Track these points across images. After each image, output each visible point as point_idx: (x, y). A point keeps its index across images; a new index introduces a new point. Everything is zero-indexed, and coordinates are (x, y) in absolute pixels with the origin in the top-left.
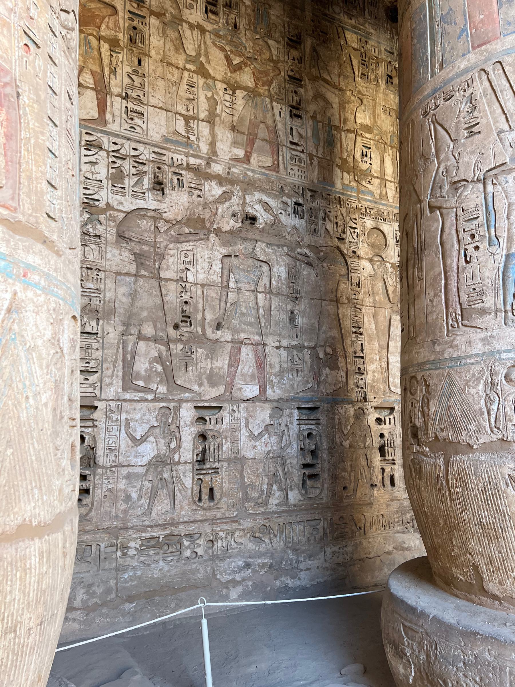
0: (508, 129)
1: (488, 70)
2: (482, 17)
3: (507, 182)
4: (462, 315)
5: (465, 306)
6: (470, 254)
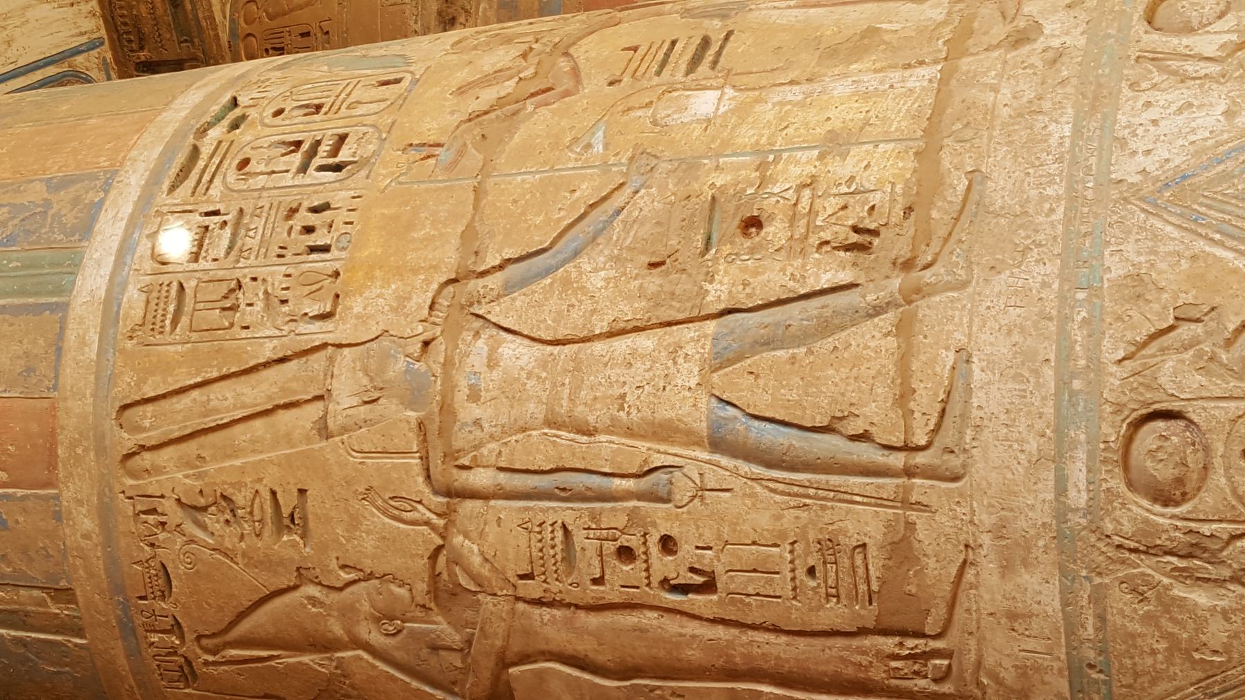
0: (320, 405)
3: (477, 423)
4: (904, 633)
5: (868, 614)
6: (683, 571)
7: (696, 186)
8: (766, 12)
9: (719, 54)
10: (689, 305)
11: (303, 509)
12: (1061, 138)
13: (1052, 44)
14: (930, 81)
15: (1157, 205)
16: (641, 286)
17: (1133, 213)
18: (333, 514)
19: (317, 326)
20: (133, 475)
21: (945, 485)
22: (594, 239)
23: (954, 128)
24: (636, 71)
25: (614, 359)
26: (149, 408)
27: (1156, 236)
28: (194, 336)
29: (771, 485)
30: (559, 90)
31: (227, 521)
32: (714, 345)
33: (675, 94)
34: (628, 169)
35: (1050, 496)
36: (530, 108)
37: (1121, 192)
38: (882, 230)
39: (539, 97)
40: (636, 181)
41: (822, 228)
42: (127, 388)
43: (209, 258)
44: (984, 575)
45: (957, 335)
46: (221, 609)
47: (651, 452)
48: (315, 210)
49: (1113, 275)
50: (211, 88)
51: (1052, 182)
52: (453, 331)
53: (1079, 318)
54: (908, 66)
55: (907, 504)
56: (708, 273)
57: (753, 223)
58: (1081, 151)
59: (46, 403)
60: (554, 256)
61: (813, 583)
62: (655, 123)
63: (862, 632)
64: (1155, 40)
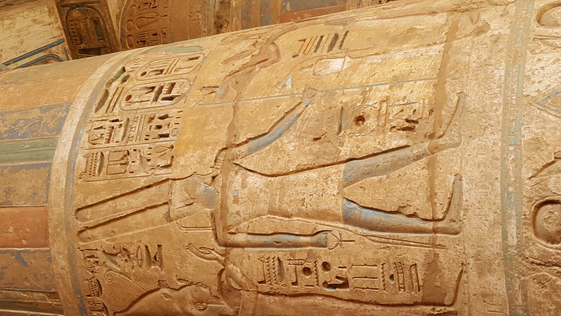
0: (166, 207)
1: (81, 226)
2: (11, 230)
3: (238, 213)
4: (435, 304)
5: (418, 296)
6: (333, 278)
7: (334, 103)
8: (363, 22)
9: (343, 41)
10: (332, 157)
11: (160, 254)
12: (500, 76)
13: (494, 33)
14: (439, 52)
15: (545, 106)
16: (310, 149)
17: (534, 110)
18: (174, 256)
19: (164, 171)
20: (83, 240)
21: (451, 236)
22: (288, 128)
23: (451, 73)
24: (305, 50)
25: (299, 183)
26: (90, 210)
27: (545, 120)
28: (109, 177)
29: (372, 238)
30: (270, 60)
31: (126, 260)
32: (344, 175)
33: (323, 61)
34: (303, 96)
35: (500, 240)
36: (257, 69)
37: (528, 101)
38: (420, 121)
39: (261, 64)
40: (306, 101)
41: (392, 121)
42: (79, 201)
43: (114, 141)
44: (471, 277)
45: (455, 168)
46: (124, 300)
47: (317, 224)
48: (161, 118)
49: (525, 139)
50: (113, 63)
51: (496, 97)
52: (225, 172)
53: (511, 159)
54: (429, 45)
55: (434, 245)
56: (340, 142)
57: (360, 119)
58: (509, 82)
59: (43, 209)
60: (270, 136)
61: (393, 282)
62: (314, 74)
63: (415, 304)
64: (541, 30)
